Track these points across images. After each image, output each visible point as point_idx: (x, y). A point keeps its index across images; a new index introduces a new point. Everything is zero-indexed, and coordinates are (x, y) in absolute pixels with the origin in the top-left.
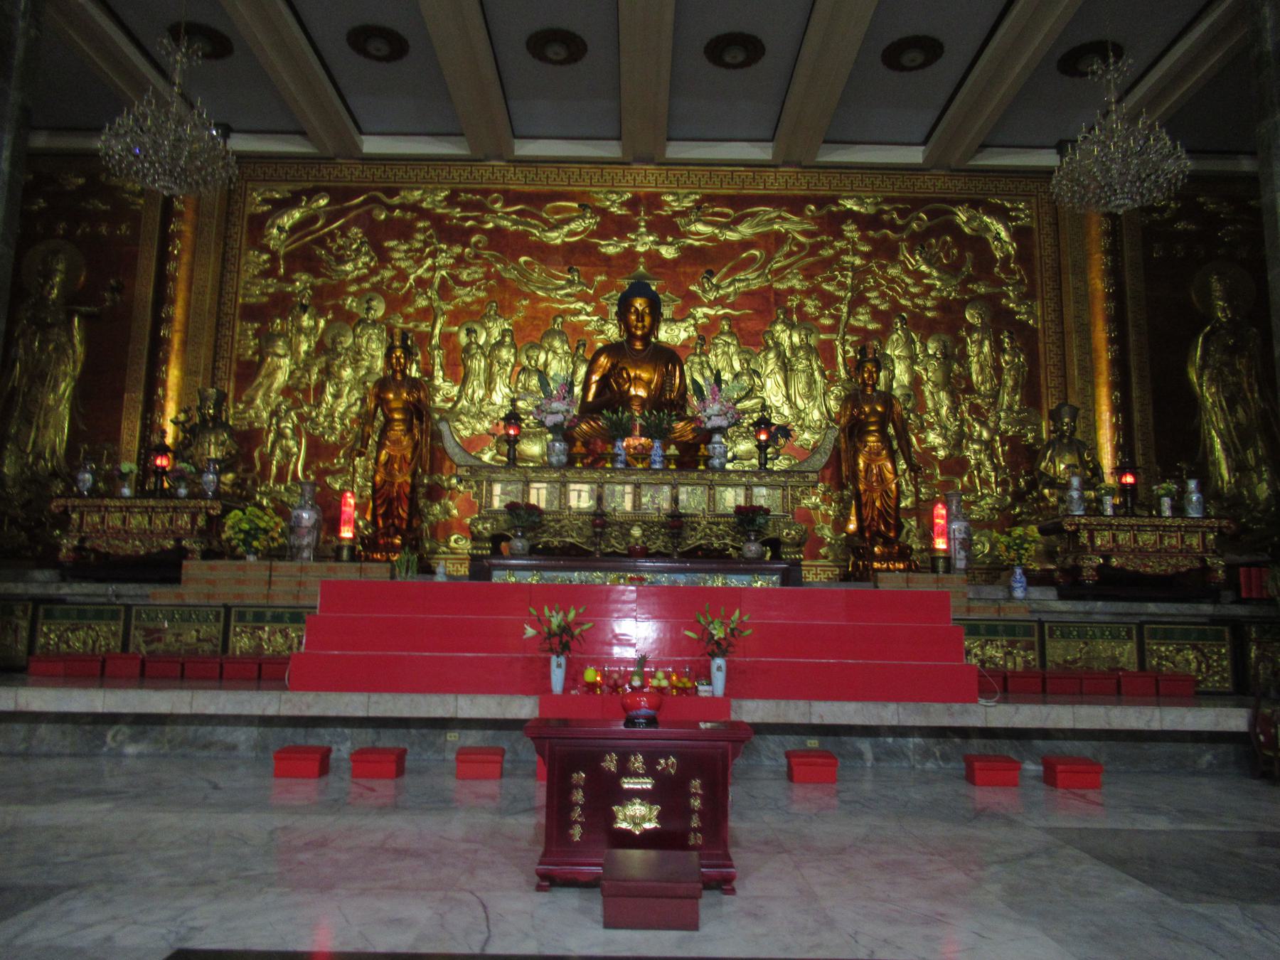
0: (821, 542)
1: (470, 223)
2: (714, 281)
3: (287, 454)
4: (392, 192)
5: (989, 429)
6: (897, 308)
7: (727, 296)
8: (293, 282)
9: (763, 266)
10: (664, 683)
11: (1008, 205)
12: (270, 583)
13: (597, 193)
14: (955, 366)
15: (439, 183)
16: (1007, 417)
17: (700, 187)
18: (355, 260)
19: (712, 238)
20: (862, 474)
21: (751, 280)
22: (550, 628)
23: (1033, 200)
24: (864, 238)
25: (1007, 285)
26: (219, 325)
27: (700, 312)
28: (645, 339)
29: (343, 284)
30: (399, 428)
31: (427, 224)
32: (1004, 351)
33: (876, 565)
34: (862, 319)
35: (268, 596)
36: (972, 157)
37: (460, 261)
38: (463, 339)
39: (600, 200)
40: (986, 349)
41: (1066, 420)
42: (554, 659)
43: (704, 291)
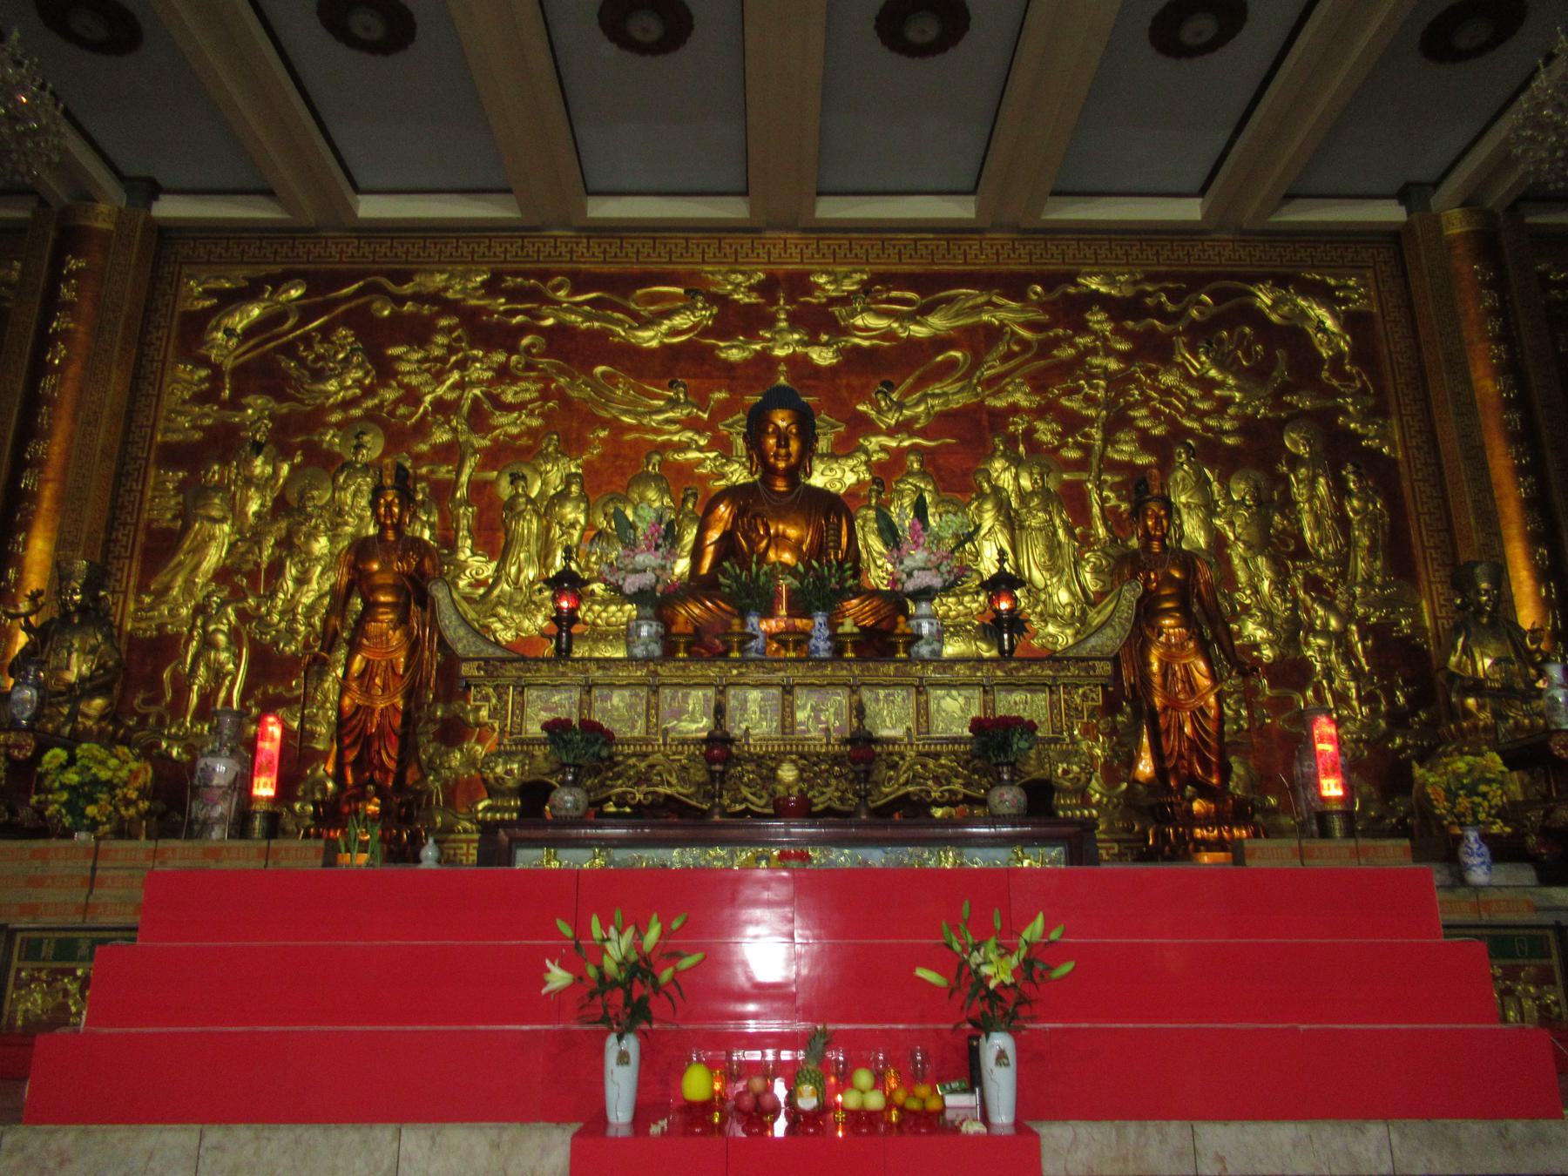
1: (519, 318)
2: (895, 396)
3: (218, 674)
4: (403, 277)
5: (1339, 615)
6: (1178, 433)
7: (915, 419)
8: (243, 408)
9: (968, 375)
10: (875, 1101)
11: (1332, 282)
12: (92, 882)
13: (712, 273)
14: (1277, 518)
15: (473, 262)
16: (1365, 594)
17: (868, 263)
18: (340, 376)
19: (888, 335)
20: (1157, 680)
21: (951, 395)
22: (600, 967)
23: (1369, 273)
24: (1119, 331)
25: (1344, 396)
26: (120, 477)
27: (873, 443)
29: (322, 411)
31: (454, 321)
32: (1349, 493)
33: (1198, 833)
35: (86, 908)
36: (1272, 214)
37: (503, 374)
38: (505, 490)
39: (717, 284)
40: (1322, 489)
41: (1484, 585)
42: (612, 1045)
43: (880, 411)
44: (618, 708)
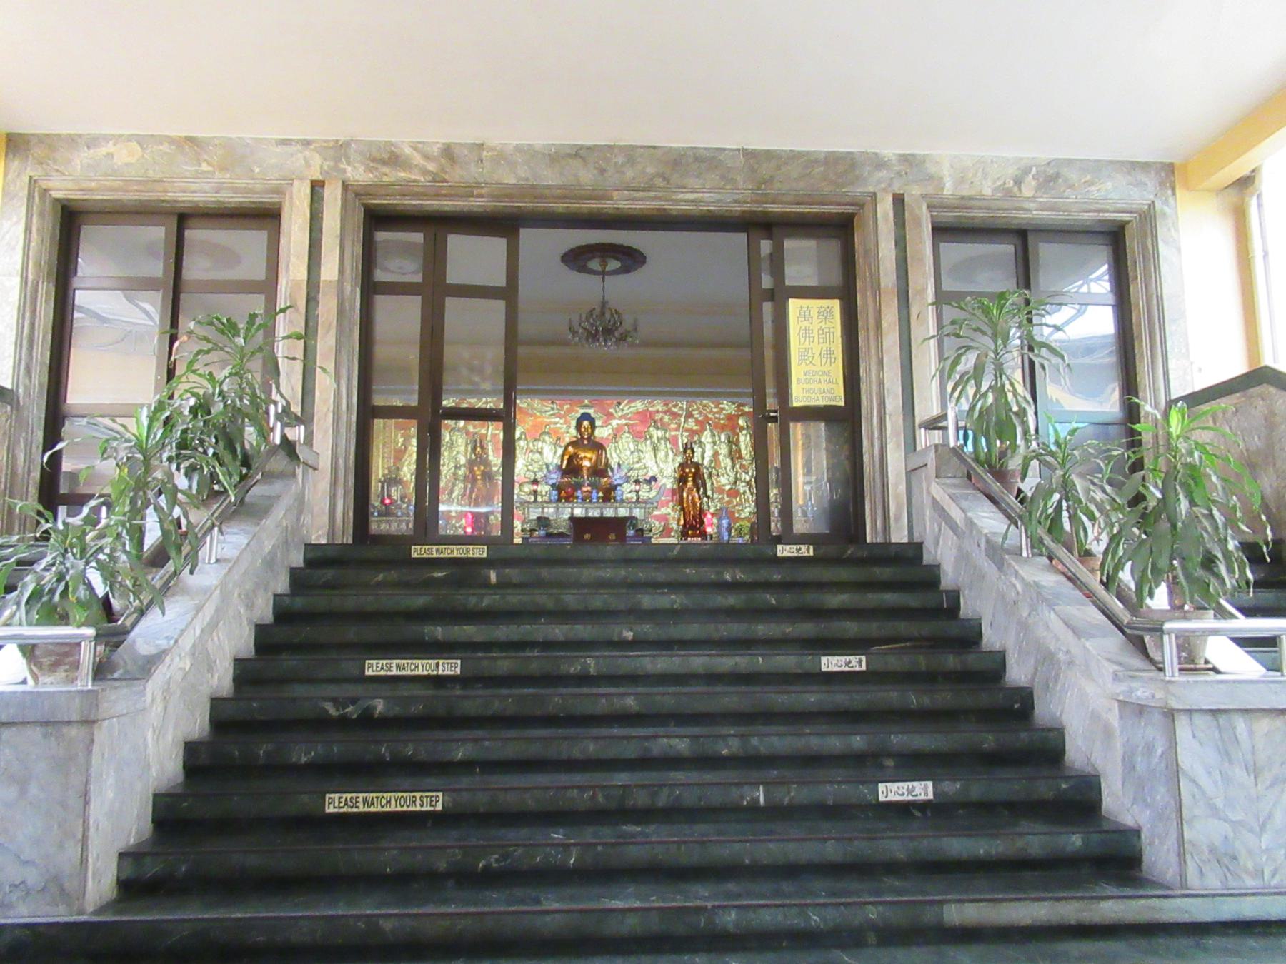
0: (672, 530)
27: (615, 423)
28: (589, 439)
30: (480, 482)
34: (691, 424)
44: (550, 511)
